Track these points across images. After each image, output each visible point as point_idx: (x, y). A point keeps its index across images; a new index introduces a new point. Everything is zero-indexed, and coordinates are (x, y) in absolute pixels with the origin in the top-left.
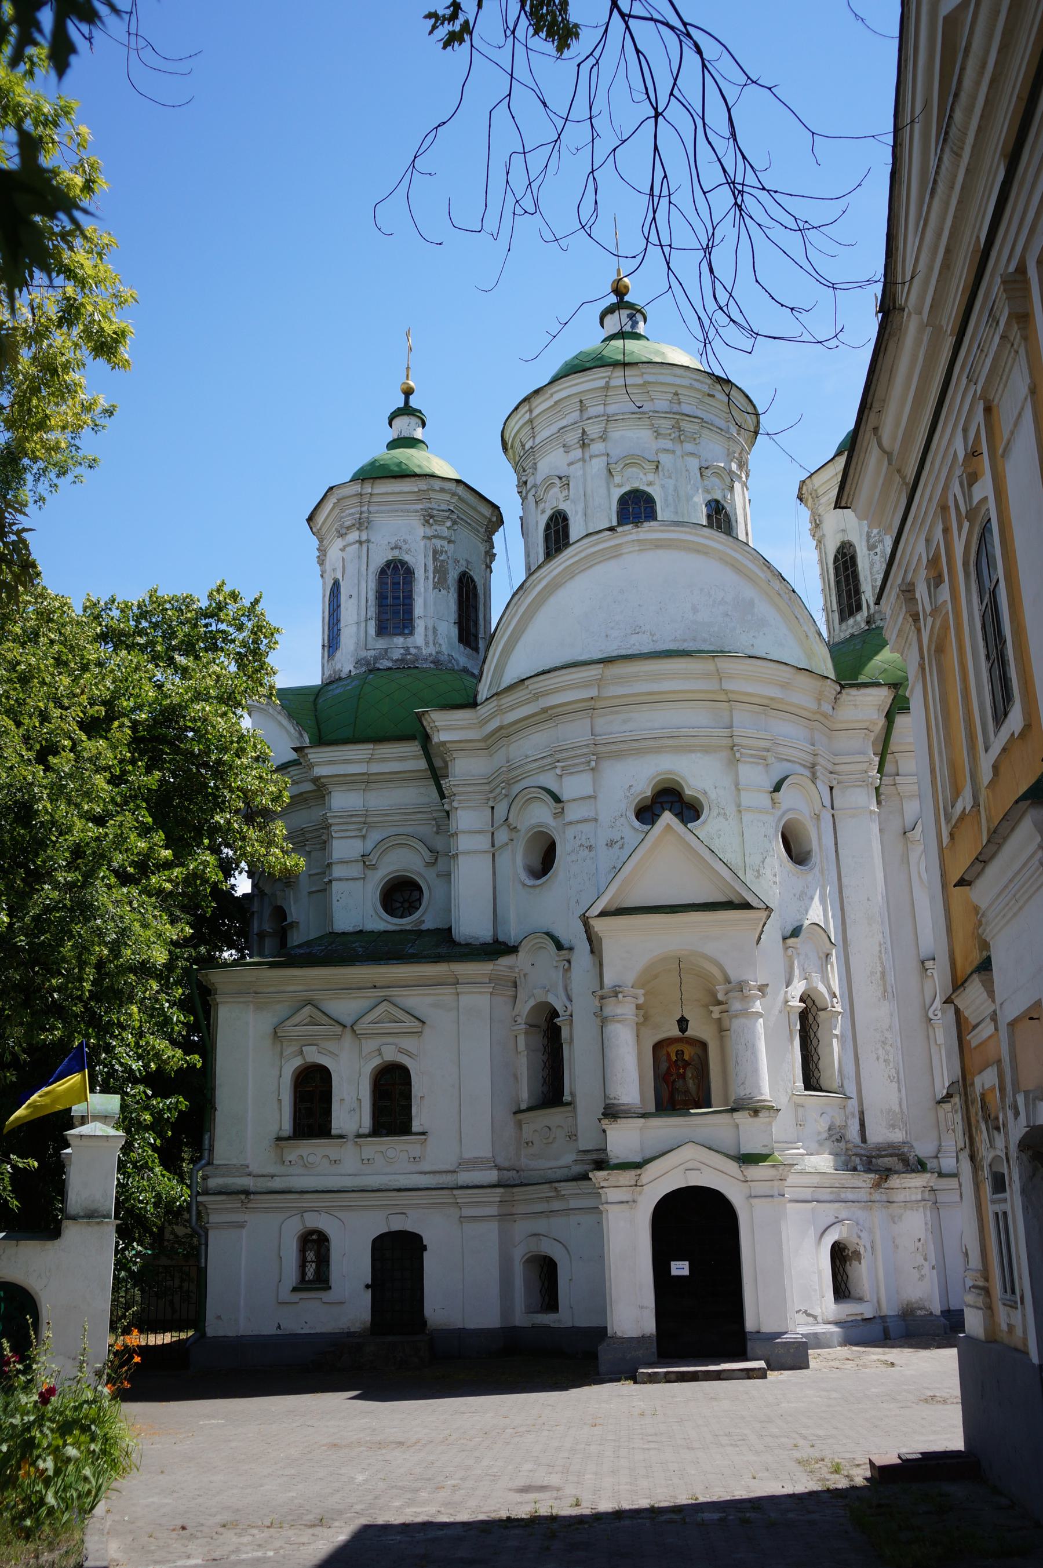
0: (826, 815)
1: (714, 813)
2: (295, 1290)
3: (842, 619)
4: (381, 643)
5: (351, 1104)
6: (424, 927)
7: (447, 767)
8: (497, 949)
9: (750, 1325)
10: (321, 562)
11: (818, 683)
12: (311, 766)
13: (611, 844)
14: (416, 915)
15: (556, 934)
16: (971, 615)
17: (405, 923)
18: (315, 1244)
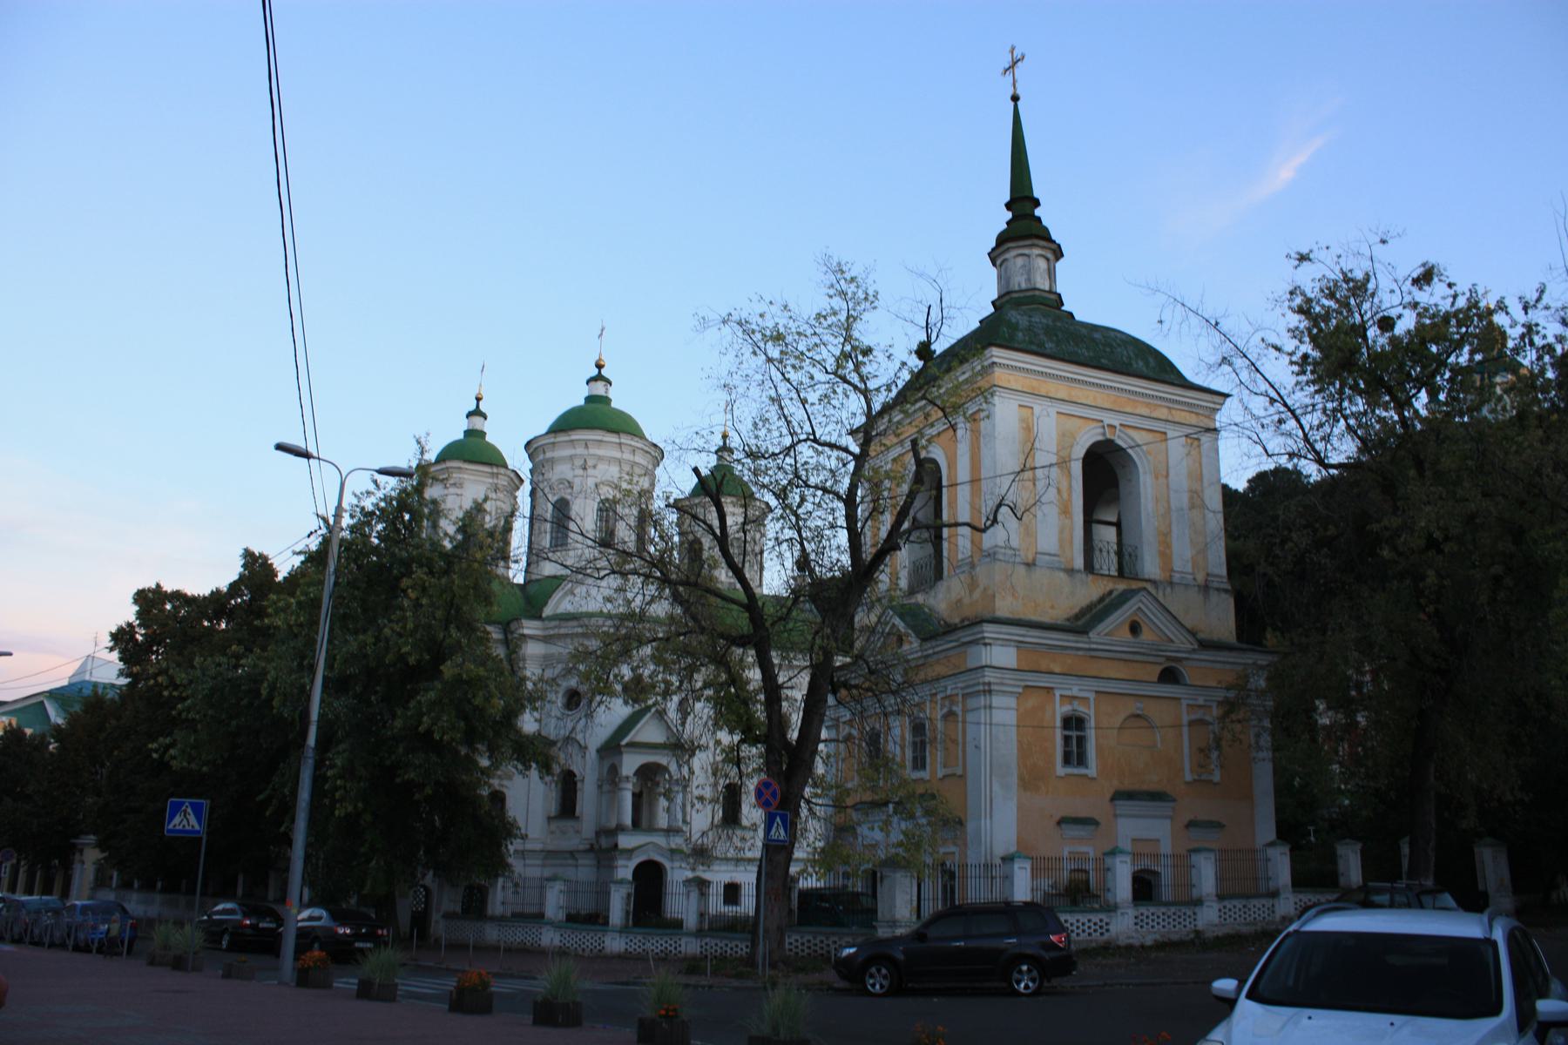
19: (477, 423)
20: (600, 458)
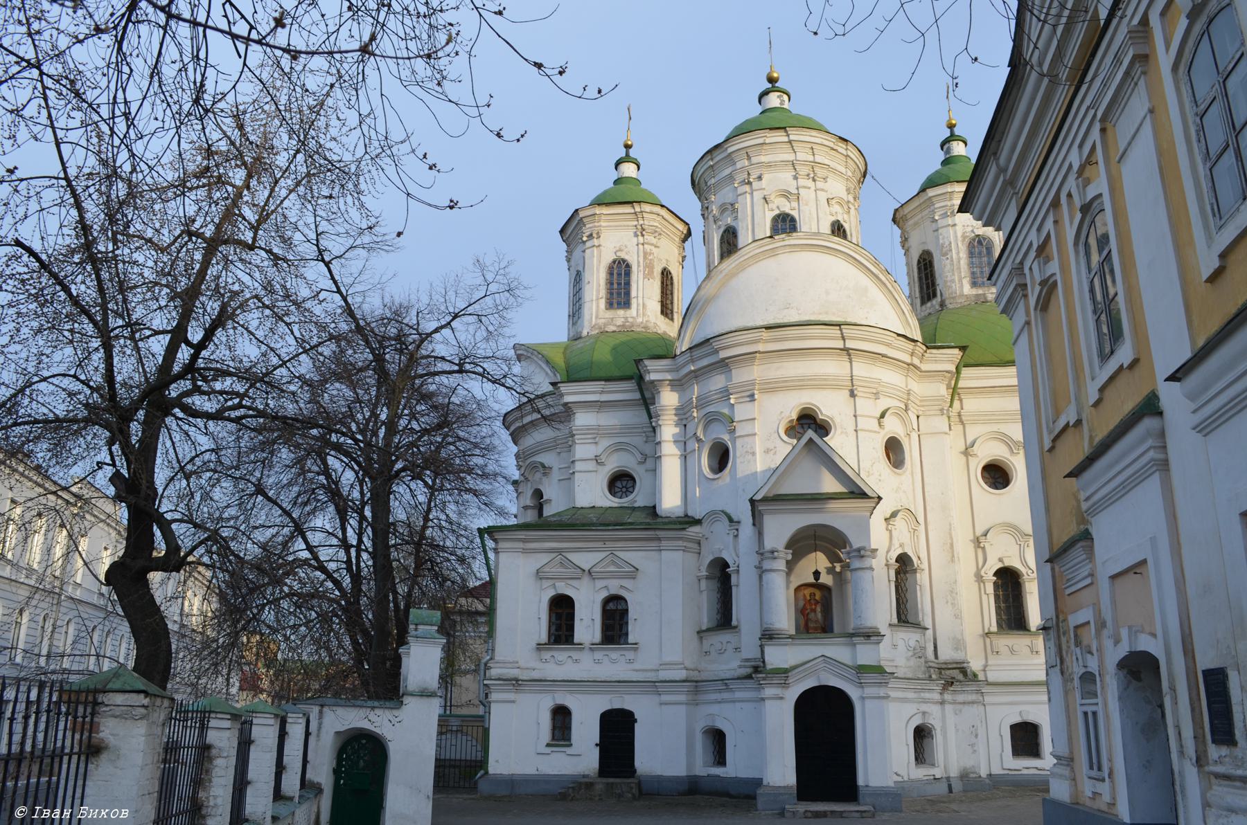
0: (914, 436)
1: (839, 431)
2: (548, 745)
3: (923, 303)
4: (610, 314)
5: (588, 624)
6: (636, 505)
7: (654, 398)
8: (688, 521)
9: (861, 781)
10: (568, 260)
11: (910, 346)
12: (562, 395)
13: (767, 451)
14: (631, 497)
15: (728, 511)
16: (1080, 282)
17: (625, 501)
18: (561, 716)
19: (629, 170)
20: (769, 165)
